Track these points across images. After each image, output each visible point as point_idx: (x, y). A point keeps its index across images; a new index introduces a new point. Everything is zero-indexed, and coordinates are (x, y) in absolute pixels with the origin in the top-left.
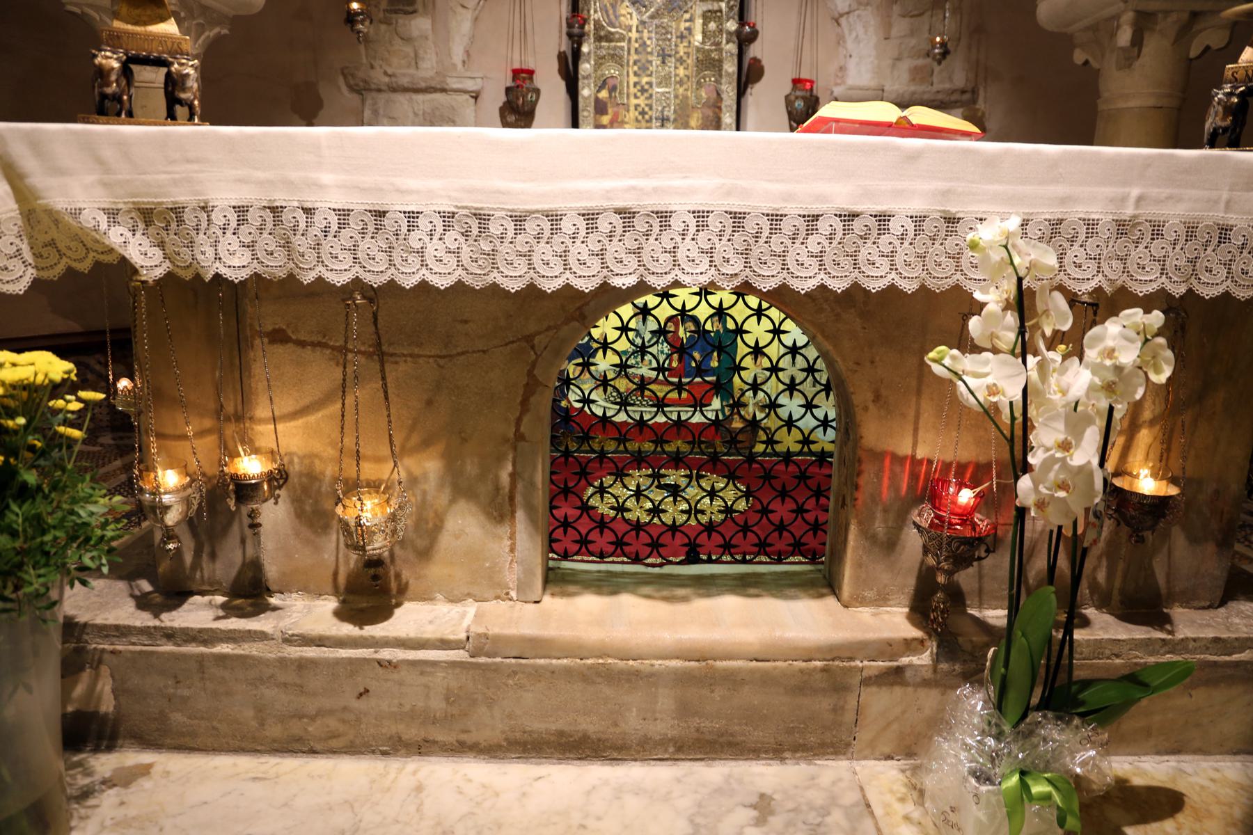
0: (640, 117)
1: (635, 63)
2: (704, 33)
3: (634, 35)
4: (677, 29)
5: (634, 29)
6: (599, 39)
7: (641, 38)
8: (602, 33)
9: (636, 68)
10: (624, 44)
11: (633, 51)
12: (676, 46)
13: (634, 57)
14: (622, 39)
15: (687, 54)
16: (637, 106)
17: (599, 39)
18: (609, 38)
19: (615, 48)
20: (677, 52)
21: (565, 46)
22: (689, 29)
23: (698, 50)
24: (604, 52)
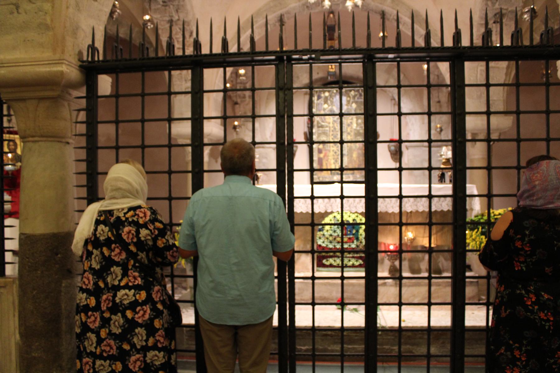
0: (335, 154)
1: (332, 135)
2: (357, 124)
3: (331, 125)
4: (347, 122)
5: (331, 123)
6: (319, 127)
7: (334, 126)
8: (320, 125)
9: (332, 137)
10: (327, 129)
11: (331, 131)
12: (347, 128)
13: (331, 133)
14: (327, 127)
15: (351, 131)
16: (333, 151)
17: (319, 127)
18: (322, 126)
19: (324, 130)
20: (347, 131)
21: (306, 130)
22: (351, 123)
23: (355, 130)
24: (320, 132)
